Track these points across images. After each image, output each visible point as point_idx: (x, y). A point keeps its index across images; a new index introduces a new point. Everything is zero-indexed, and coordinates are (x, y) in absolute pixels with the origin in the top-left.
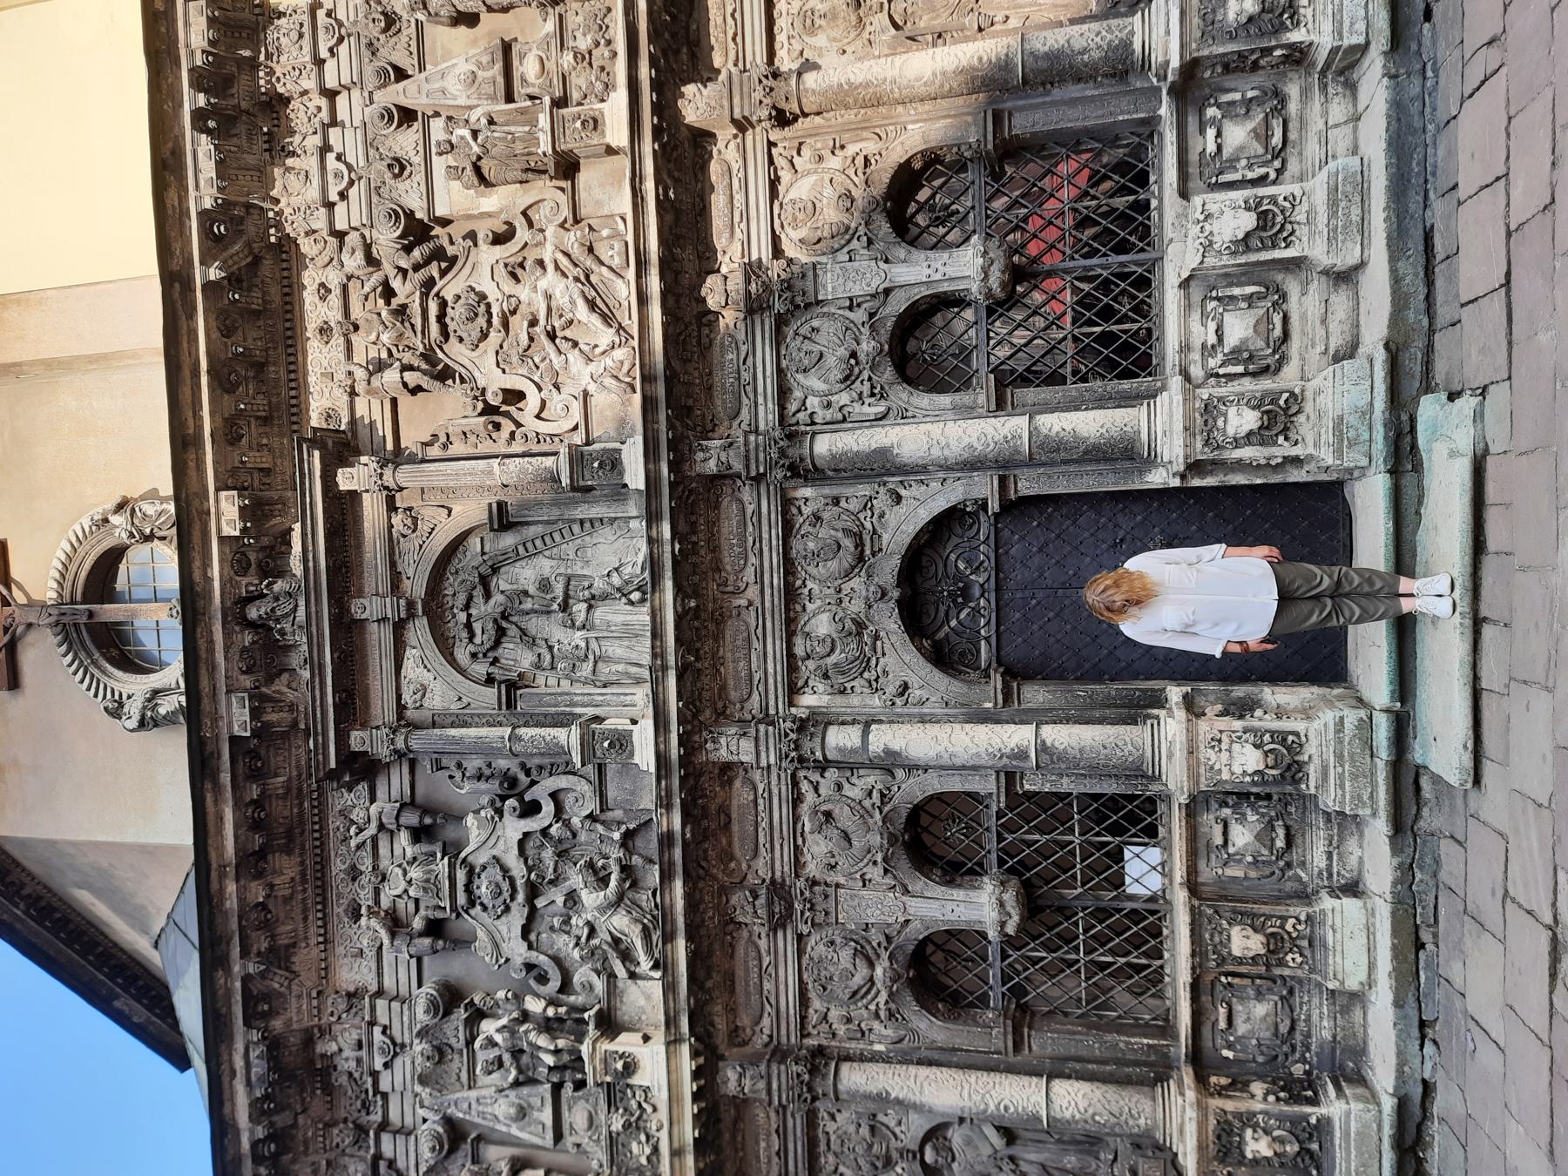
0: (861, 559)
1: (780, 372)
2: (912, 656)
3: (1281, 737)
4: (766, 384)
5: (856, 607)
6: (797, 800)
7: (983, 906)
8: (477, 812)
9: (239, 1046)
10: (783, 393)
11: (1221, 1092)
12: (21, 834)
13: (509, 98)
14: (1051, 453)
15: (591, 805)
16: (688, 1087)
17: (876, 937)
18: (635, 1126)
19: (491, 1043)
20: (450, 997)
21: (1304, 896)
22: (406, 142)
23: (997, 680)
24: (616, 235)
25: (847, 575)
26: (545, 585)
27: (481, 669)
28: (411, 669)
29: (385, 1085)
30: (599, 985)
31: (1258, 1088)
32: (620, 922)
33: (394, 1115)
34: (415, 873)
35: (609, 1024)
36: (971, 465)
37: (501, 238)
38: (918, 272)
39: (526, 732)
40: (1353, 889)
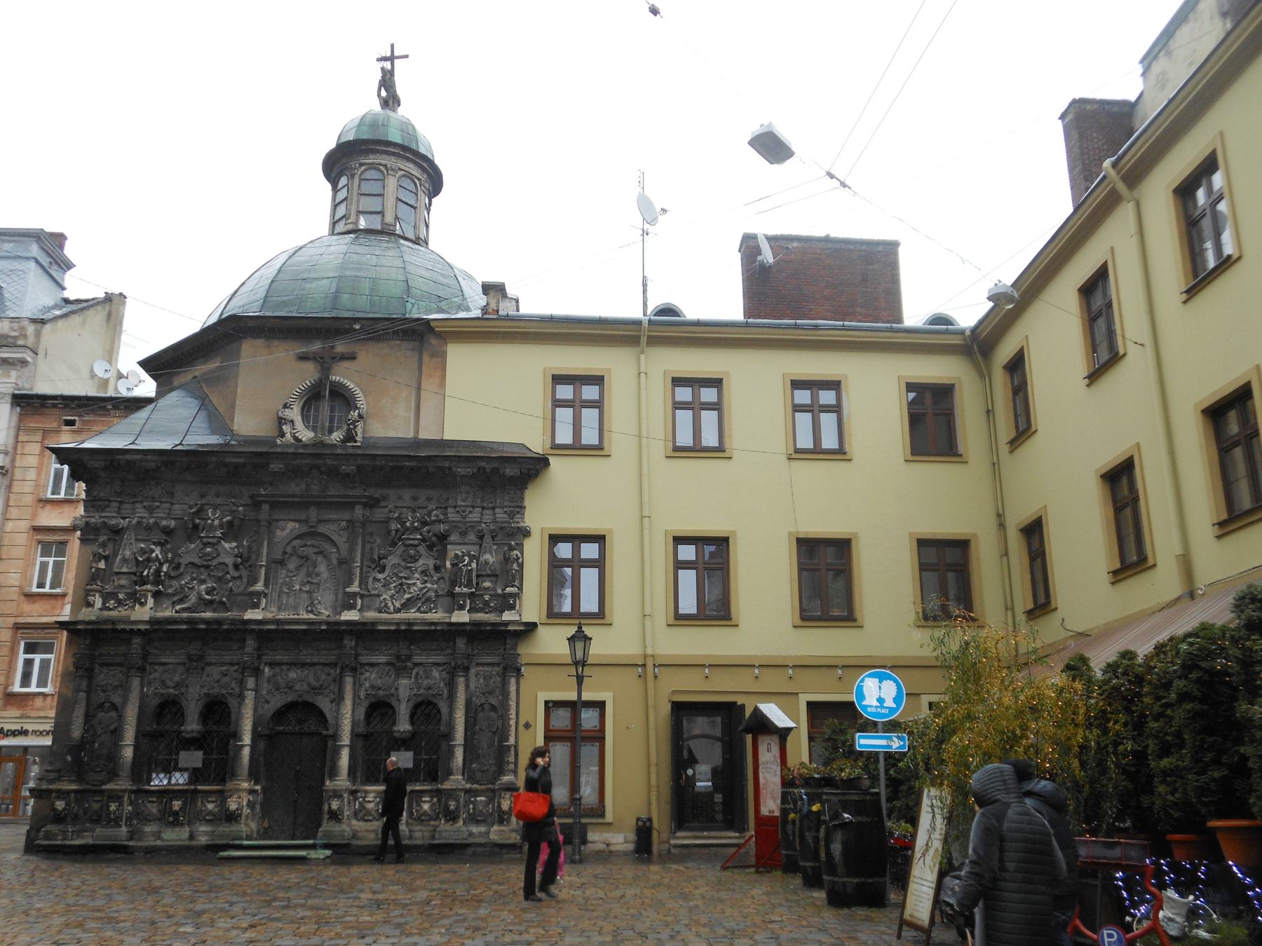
0: (314, 688)
1: (378, 664)
2: (279, 705)
3: (240, 815)
4: (374, 659)
5: (297, 687)
6: (232, 664)
7: (192, 726)
8: (237, 547)
9: (156, 458)
10: (372, 665)
11: (129, 797)
12: (243, 353)
13: (478, 576)
14: (337, 751)
15: (236, 590)
16: (135, 627)
17: (183, 690)
18: (120, 603)
19: (153, 551)
20: (168, 532)
21: (189, 824)
22: (472, 537)
23: (267, 732)
24: (430, 610)
25: (309, 685)
26: (318, 575)
27: (289, 550)
28: (291, 525)
29: (138, 505)
30: (170, 591)
31: (130, 808)
32: (193, 598)
33: (125, 506)
34: (216, 522)
35: (157, 595)
36: (338, 726)
37: (437, 569)
38: (403, 711)
39: (263, 571)
40: (191, 837)
